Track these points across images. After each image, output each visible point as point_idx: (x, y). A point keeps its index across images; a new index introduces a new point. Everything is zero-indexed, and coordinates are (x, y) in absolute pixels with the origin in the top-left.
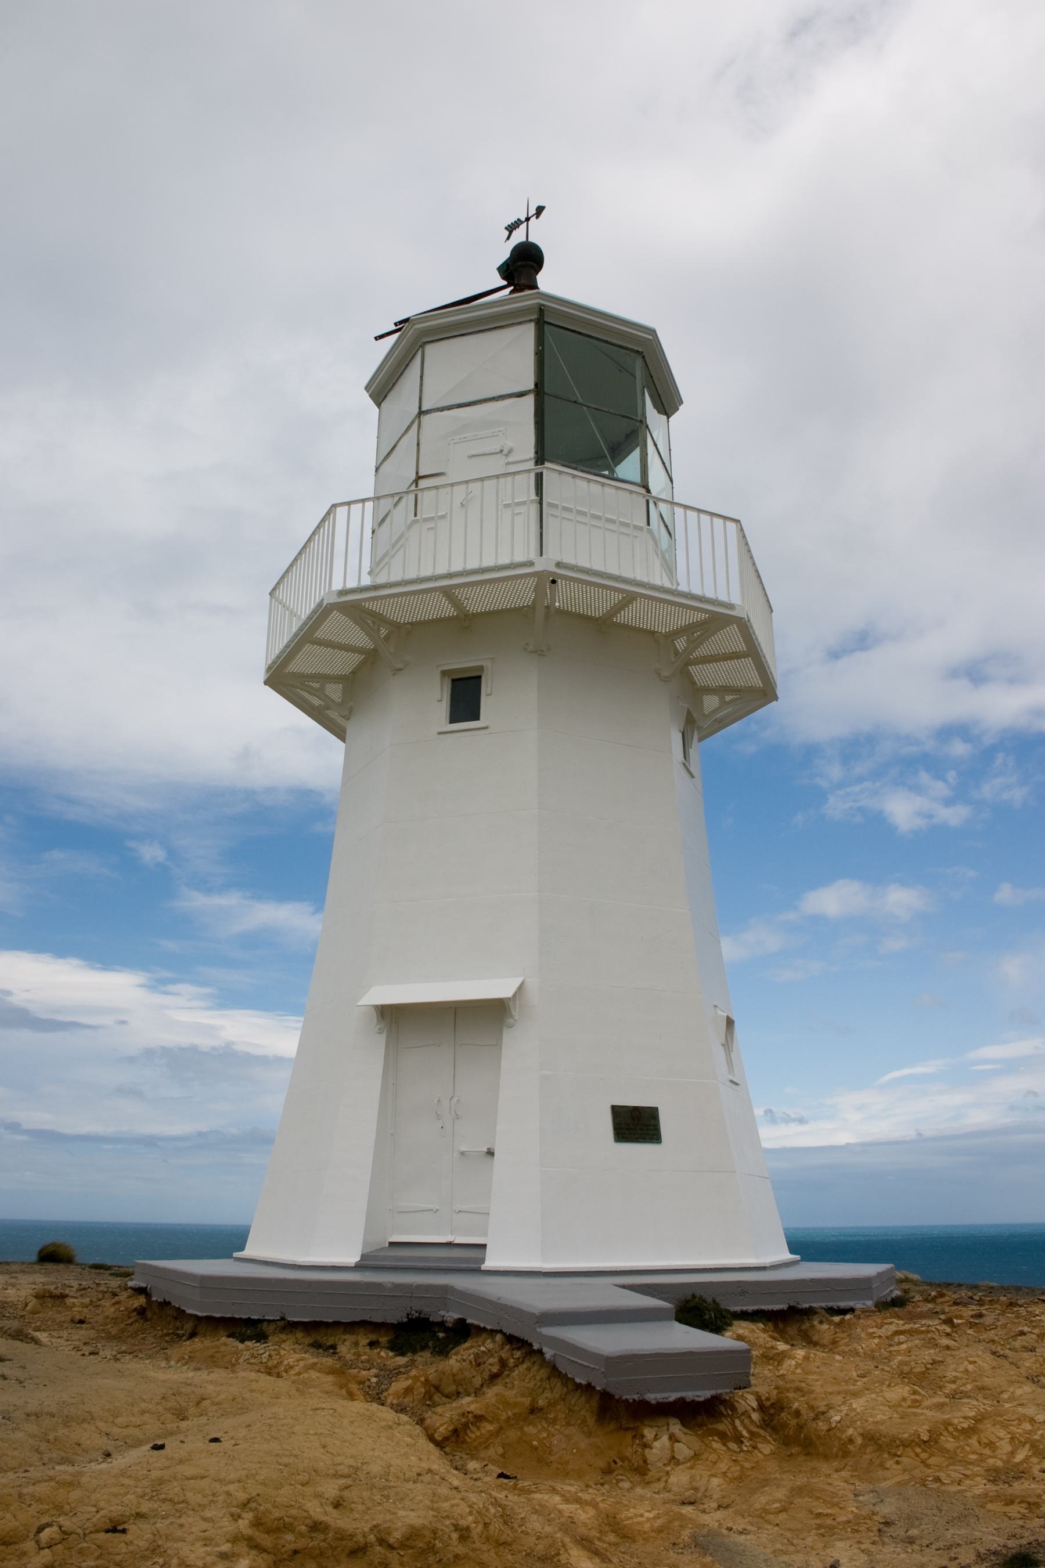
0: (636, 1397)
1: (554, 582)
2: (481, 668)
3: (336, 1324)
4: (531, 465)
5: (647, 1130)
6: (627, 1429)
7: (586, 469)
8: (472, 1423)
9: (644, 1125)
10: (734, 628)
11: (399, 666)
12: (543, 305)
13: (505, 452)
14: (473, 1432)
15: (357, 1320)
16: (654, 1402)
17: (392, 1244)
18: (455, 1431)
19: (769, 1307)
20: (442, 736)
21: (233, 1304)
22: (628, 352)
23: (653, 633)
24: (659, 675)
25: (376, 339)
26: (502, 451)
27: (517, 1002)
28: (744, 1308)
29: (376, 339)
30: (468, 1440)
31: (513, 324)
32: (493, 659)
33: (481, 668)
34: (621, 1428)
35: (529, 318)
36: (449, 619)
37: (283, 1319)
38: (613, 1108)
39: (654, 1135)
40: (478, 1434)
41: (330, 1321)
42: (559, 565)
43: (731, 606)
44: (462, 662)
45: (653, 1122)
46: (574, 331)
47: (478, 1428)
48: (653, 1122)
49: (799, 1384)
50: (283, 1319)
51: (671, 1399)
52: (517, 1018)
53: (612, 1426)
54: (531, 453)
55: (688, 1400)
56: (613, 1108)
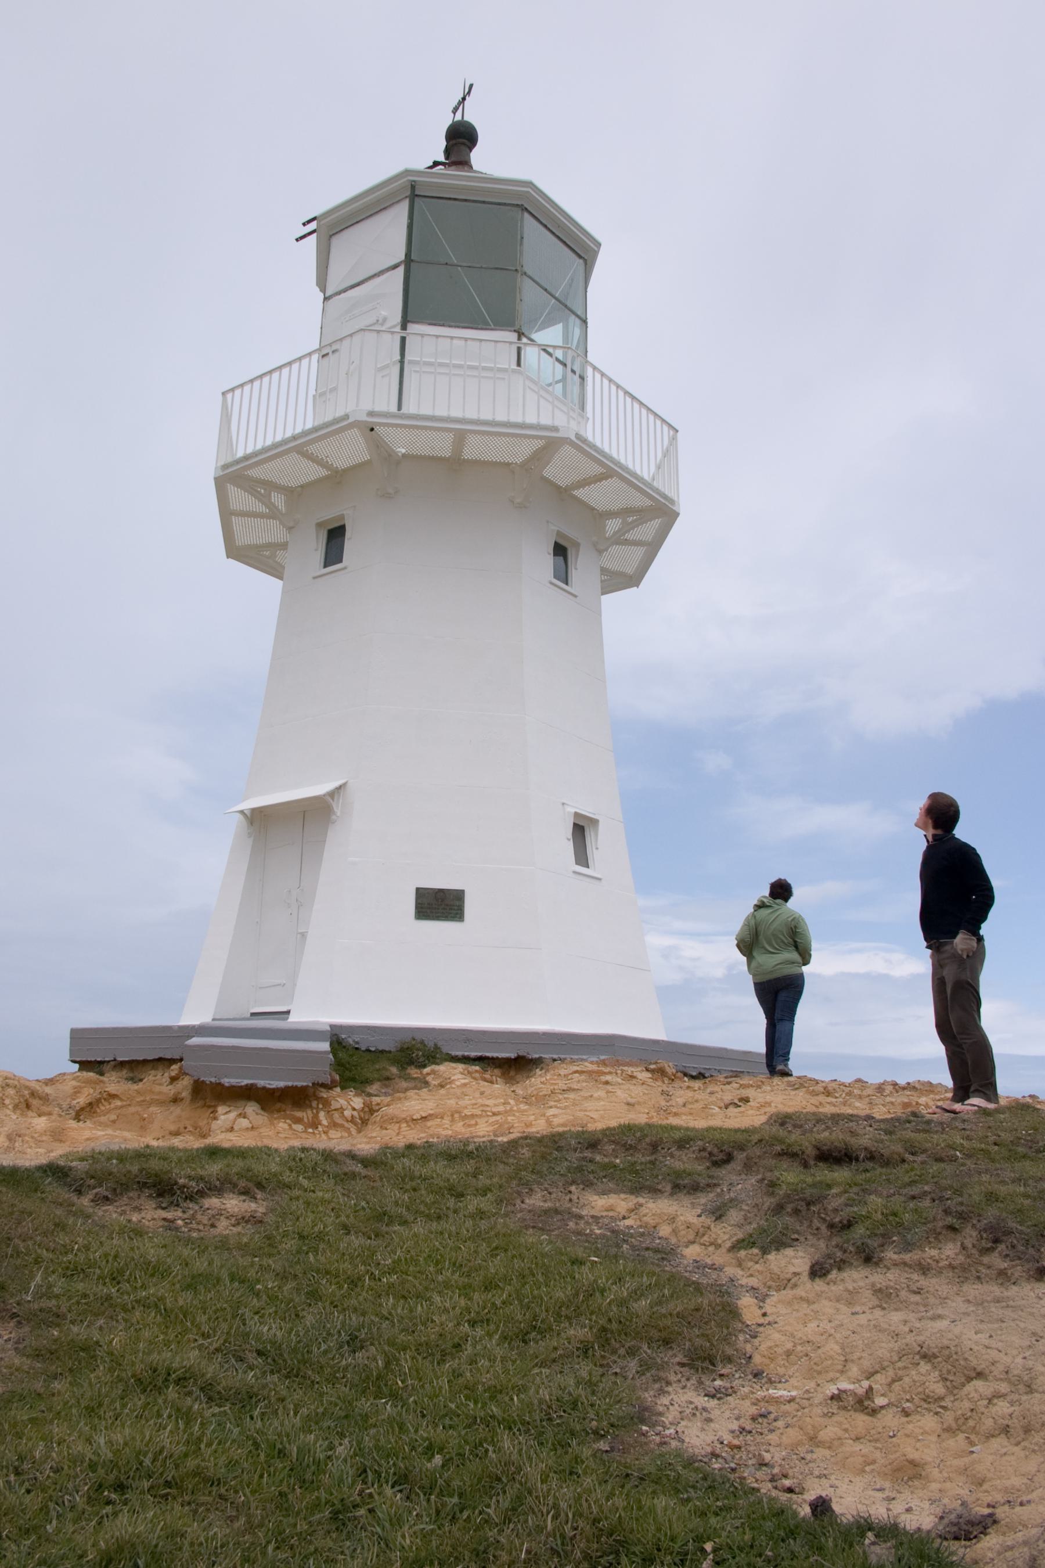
0: (213, 1080)
1: (372, 430)
2: (342, 517)
3: (145, 1062)
4: (398, 329)
5: (451, 909)
6: (209, 1107)
7: (453, 324)
8: (105, 1099)
9: (447, 905)
10: (567, 450)
11: (291, 524)
12: (414, 181)
13: (381, 321)
14: (103, 1105)
15: (157, 1057)
16: (227, 1085)
17: (253, 1014)
18: (90, 1104)
19: (495, 1055)
20: (316, 580)
21: (88, 1050)
22: (509, 208)
23: (508, 464)
24: (513, 502)
25: (297, 240)
26: (378, 321)
27: (341, 801)
28: (466, 1054)
29: (297, 240)
30: (98, 1111)
31: (393, 204)
32: (355, 507)
33: (342, 517)
34: (204, 1106)
35: (404, 196)
36: (327, 478)
37: (115, 1060)
38: (418, 889)
39: (457, 914)
40: (108, 1107)
41: (141, 1059)
42: (371, 414)
43: (556, 429)
44: (329, 514)
45: (457, 903)
46: (450, 199)
47: (110, 1104)
48: (457, 903)
49: (849, 1209)
50: (115, 1060)
51: (243, 1084)
52: (339, 814)
53: (201, 1103)
54: (398, 318)
55: (259, 1086)
56: (418, 889)
